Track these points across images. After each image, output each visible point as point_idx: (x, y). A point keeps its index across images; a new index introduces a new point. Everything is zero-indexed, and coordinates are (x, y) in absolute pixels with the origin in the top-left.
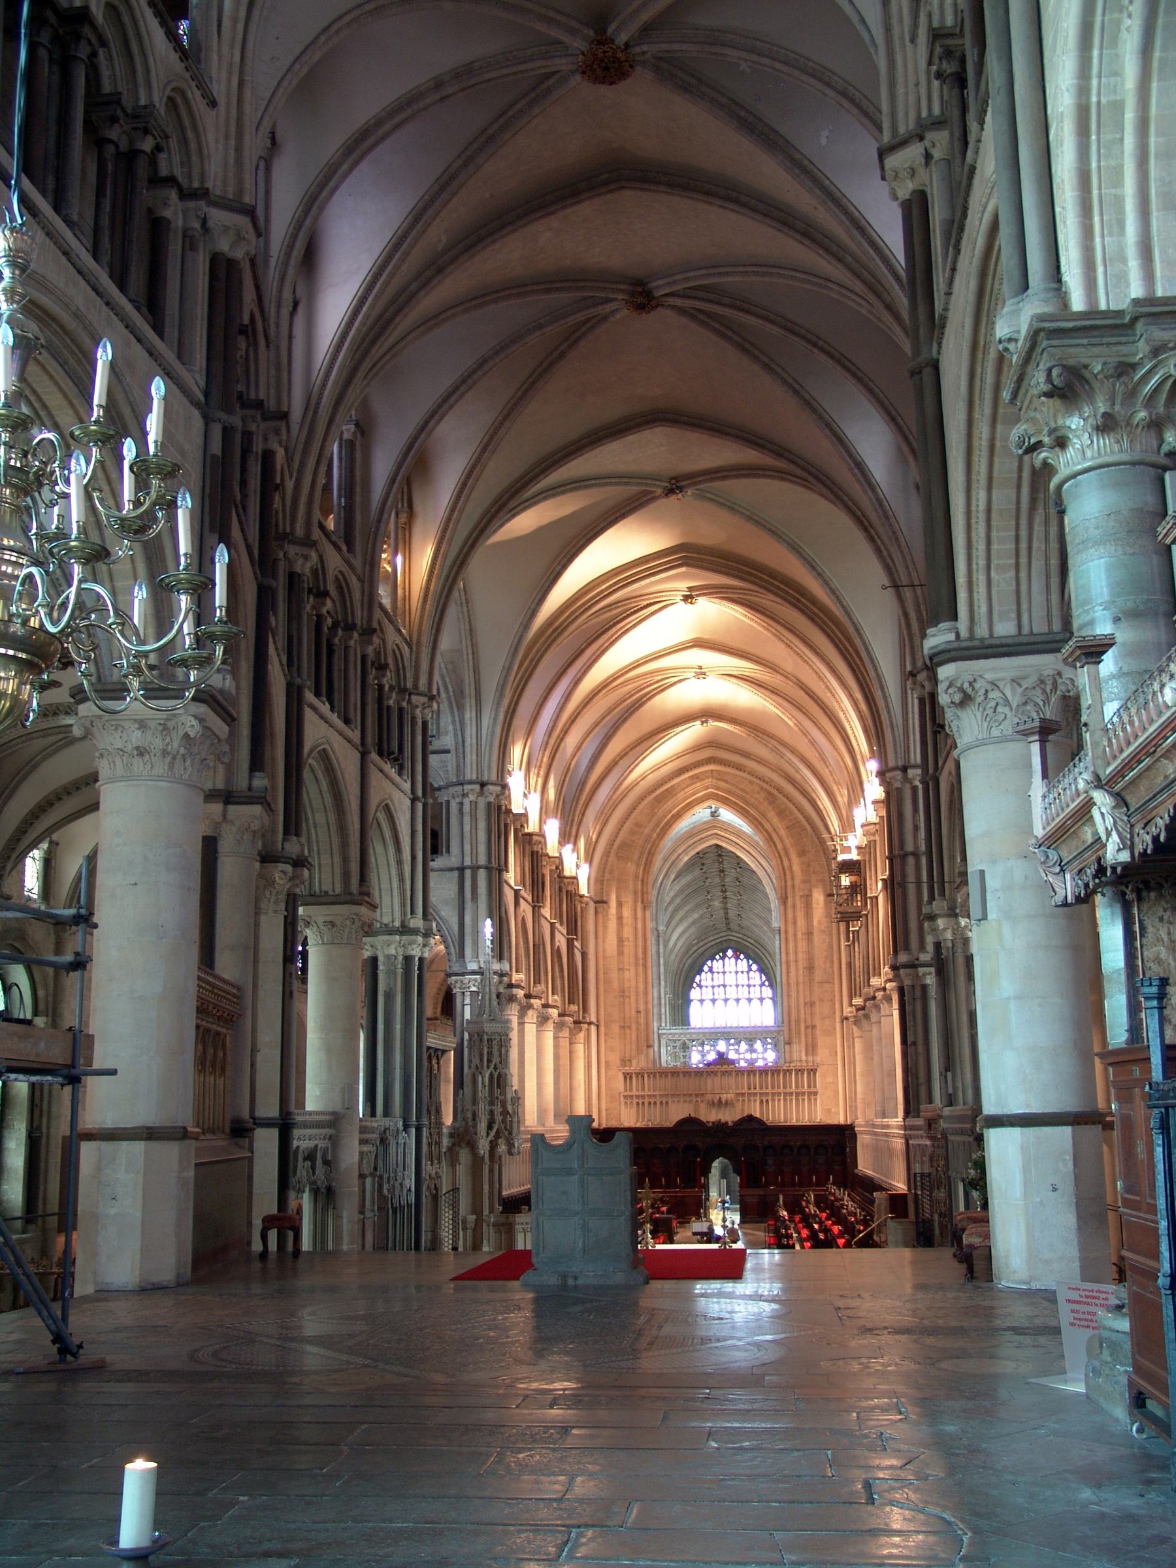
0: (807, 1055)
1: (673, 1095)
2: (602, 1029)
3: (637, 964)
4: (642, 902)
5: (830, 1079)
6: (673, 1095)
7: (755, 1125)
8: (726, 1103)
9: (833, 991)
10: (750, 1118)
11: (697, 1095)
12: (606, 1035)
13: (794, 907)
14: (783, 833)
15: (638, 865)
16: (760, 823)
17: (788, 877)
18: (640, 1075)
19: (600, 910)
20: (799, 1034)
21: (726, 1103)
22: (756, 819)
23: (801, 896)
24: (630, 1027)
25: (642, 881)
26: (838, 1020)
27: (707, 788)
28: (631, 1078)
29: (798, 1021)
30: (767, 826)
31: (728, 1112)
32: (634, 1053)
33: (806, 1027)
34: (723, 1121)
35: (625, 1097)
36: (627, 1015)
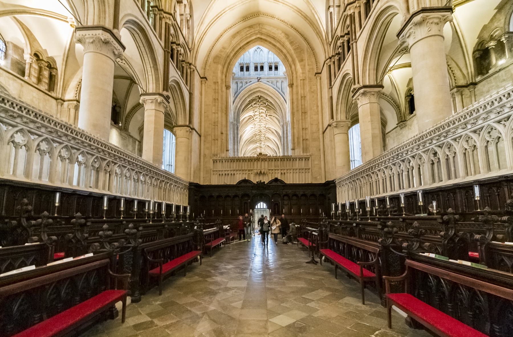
0: (303, 152)
2: (202, 138)
3: (222, 112)
4: (226, 86)
5: (316, 162)
7: (279, 184)
8: (264, 173)
9: (318, 120)
10: (276, 180)
11: (249, 171)
12: (204, 141)
13: (297, 86)
14: (292, 52)
15: (224, 67)
16: (282, 51)
17: (294, 73)
18: (221, 161)
19: (203, 82)
20: (299, 143)
21: (264, 173)
22: (280, 49)
23: (301, 80)
24: (217, 140)
25: (226, 76)
28: (217, 162)
29: (298, 138)
30: (284, 51)
31: (265, 178)
32: (219, 152)
33: (303, 140)
34: (262, 181)
35: (213, 171)
36: (216, 134)
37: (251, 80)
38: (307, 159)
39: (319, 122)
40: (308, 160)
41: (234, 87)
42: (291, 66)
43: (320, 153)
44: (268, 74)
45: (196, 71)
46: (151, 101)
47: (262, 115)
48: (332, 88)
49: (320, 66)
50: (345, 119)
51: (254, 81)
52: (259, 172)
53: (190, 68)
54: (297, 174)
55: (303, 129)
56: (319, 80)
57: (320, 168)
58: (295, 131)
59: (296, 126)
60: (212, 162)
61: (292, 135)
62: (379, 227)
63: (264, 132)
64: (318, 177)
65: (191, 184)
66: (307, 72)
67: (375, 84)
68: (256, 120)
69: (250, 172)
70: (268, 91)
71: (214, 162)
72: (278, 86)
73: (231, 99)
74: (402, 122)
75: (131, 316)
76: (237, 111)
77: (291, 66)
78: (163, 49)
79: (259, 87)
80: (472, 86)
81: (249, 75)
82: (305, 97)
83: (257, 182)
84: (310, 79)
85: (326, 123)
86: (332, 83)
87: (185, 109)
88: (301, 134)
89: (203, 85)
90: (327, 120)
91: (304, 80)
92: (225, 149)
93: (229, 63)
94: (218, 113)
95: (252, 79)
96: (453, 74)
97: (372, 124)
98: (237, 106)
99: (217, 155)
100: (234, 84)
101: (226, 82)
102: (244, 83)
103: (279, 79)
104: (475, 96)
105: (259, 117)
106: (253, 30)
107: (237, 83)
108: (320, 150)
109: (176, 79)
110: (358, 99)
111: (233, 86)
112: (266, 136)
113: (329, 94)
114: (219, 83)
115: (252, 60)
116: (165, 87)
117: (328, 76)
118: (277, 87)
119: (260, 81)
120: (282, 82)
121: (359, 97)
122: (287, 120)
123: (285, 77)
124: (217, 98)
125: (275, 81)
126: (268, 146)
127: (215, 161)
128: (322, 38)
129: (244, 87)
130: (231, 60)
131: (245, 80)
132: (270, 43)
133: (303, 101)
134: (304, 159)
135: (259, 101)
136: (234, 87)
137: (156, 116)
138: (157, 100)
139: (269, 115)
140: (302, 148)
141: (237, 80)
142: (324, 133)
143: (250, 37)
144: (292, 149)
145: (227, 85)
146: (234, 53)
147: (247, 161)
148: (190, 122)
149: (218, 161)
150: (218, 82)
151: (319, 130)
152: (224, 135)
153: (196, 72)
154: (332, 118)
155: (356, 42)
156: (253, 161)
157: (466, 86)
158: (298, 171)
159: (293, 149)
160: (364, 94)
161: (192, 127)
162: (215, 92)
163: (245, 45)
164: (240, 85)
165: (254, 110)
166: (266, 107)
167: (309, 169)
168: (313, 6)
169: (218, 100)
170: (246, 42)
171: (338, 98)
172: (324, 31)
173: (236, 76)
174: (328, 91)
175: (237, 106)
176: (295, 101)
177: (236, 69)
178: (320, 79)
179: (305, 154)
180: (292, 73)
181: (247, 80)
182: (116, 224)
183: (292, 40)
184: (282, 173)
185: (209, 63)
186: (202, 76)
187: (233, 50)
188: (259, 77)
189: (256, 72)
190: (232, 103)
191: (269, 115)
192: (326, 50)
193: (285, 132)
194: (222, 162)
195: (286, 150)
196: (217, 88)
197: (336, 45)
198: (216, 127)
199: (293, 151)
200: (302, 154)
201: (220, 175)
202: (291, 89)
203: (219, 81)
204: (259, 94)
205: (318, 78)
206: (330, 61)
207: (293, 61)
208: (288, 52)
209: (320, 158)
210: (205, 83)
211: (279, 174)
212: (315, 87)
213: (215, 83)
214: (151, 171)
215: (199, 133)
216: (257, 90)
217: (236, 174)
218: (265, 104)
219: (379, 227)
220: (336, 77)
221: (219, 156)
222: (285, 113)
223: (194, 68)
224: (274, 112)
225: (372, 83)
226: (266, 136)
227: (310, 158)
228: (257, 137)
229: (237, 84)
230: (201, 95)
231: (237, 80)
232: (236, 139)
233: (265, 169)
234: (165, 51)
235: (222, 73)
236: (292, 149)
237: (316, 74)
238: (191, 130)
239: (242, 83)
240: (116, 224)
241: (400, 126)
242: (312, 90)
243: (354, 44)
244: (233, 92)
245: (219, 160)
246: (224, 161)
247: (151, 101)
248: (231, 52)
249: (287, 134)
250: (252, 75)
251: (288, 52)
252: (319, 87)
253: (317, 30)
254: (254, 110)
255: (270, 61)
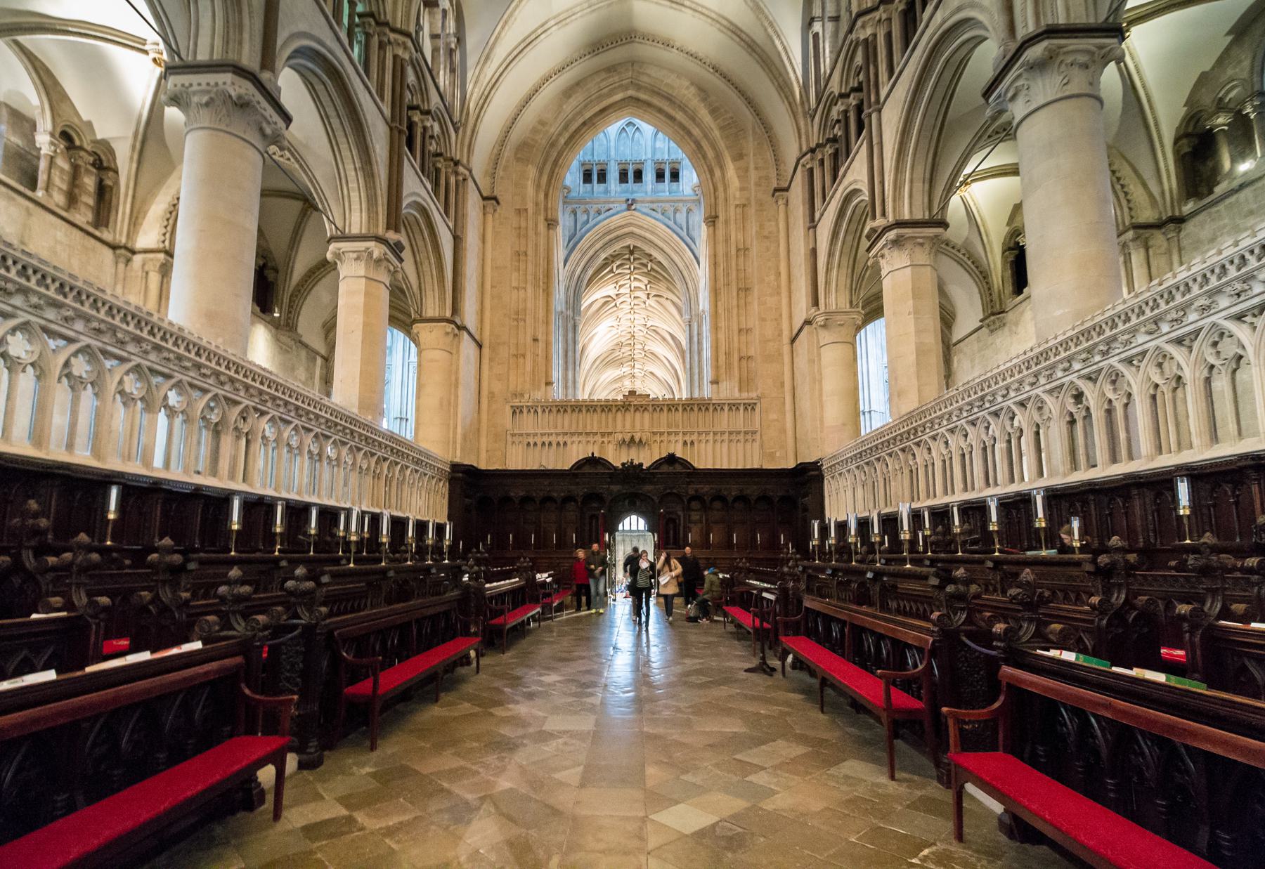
0: (740, 390)
1: (572, 434)
2: (486, 350)
3: (536, 286)
4: (546, 220)
5: (773, 416)
6: (572, 434)
7: (678, 468)
8: (640, 441)
9: (778, 309)
10: (671, 459)
11: (603, 435)
12: (491, 360)
13: (727, 222)
15: (541, 173)
16: (689, 133)
17: (721, 189)
18: (533, 409)
19: (490, 210)
20: (729, 366)
21: (640, 441)
23: (737, 206)
24: (524, 356)
25: (546, 195)
26: (786, 339)
27: (627, 89)
28: (521, 411)
30: (696, 132)
32: (527, 386)
33: (741, 359)
34: (636, 462)
35: (513, 435)
37: (611, 206)
38: (750, 407)
39: (781, 315)
40: (753, 409)
41: (567, 223)
42: (711, 172)
43: (784, 393)
44: (654, 191)
45: (470, 180)
46: (355, 255)
47: (638, 294)
48: (815, 227)
49: (785, 171)
50: (848, 305)
51: (619, 209)
52: (627, 439)
53: (457, 173)
54: (725, 445)
55: (740, 331)
56: (782, 208)
57: (783, 431)
58: (721, 336)
59: (722, 324)
60: (509, 411)
61: (711, 347)
62: (934, 581)
63: (642, 339)
64: (778, 454)
65: (455, 467)
66: (753, 187)
67: (927, 217)
68: (622, 306)
69: (605, 440)
70: (653, 233)
71: (514, 412)
72: (679, 221)
73: (560, 253)
74: (993, 314)
75: (296, 803)
76: (574, 283)
77: (711, 172)
78: (387, 123)
79: (630, 224)
80: (1171, 226)
81: (607, 191)
82: (746, 249)
83: (623, 464)
84: (760, 204)
85: (800, 316)
86: (817, 215)
87: (443, 277)
88: (736, 345)
89: (489, 217)
90: (802, 309)
91: (744, 206)
92: (544, 381)
93: (556, 163)
94: (525, 289)
95: (613, 202)
96: (1126, 194)
97: (916, 319)
98: (573, 272)
99: (522, 395)
100: (567, 215)
101: (546, 209)
102: (592, 213)
103: (681, 205)
104: (1180, 250)
105: (629, 300)
106: (616, 78)
107: (574, 212)
108: (782, 384)
109: (419, 200)
110: (882, 256)
111: (565, 221)
112: (646, 348)
113: (807, 243)
114: (530, 211)
115: (613, 153)
116: (393, 221)
117: (807, 196)
118: (675, 223)
119: (633, 207)
120: (689, 211)
121: (886, 251)
122: (701, 308)
123: (696, 198)
124: (523, 249)
125: (672, 209)
126: (651, 373)
127: (517, 411)
128: (791, 100)
129: (591, 223)
130: (560, 154)
131: (595, 206)
132: (660, 111)
133: (741, 260)
134: (742, 408)
135: (629, 259)
136: (567, 223)
137: (367, 294)
138: (371, 254)
139: (655, 296)
140: (737, 379)
141: (575, 206)
142: (793, 341)
143: (610, 95)
144: (713, 382)
145: (549, 217)
146: (567, 135)
147: (599, 410)
148: (455, 309)
149: (525, 410)
150: (526, 210)
151: (780, 335)
152: (541, 345)
153: (470, 183)
154: (816, 303)
155: (880, 111)
156: (614, 409)
157: (1158, 226)
158: (726, 437)
159: (715, 382)
160: (897, 243)
161: (459, 323)
162: (519, 236)
163: (596, 115)
164: (582, 218)
165: (616, 283)
166: (647, 274)
167: (754, 432)
168: (771, 19)
169: (526, 255)
170: (597, 108)
171: (831, 254)
172: (798, 82)
173: (573, 194)
174: (807, 236)
175: (573, 272)
176: (721, 259)
177: (572, 177)
178: (787, 204)
179: (745, 395)
180: (715, 190)
181: (599, 206)
182: (263, 567)
183: (717, 104)
184: (685, 443)
185: (503, 162)
186: (485, 194)
187: (566, 128)
188: (631, 197)
189: (624, 185)
190: (561, 264)
191: (655, 296)
192: (803, 131)
193: (695, 339)
194: (536, 411)
195: (696, 384)
196: (523, 224)
197: (827, 117)
198: (522, 323)
199: (715, 386)
200: (737, 395)
201: (529, 444)
202: (711, 228)
203: (530, 207)
204: (629, 242)
205: (780, 202)
206: (812, 159)
207: (719, 157)
208: (706, 136)
209: (784, 404)
210: (495, 210)
211: (680, 445)
212: (773, 223)
213: (519, 211)
214: (355, 434)
215: (477, 337)
216: (626, 230)
217: (569, 443)
218: (646, 266)
219: (934, 581)
220: (827, 199)
221: (527, 396)
222: (696, 290)
223: (467, 173)
224: (668, 288)
225: (918, 216)
226: (646, 348)
227: (758, 405)
228: (623, 350)
229: (575, 215)
230: (484, 242)
231: (575, 206)
232: (570, 354)
233: (642, 431)
234: (391, 129)
235: (538, 186)
236: (713, 382)
237: (776, 190)
238: (456, 331)
239: (586, 212)
240: (263, 567)
241: (989, 326)
242: (766, 233)
243: (874, 116)
244: (564, 236)
245: (527, 407)
246: (539, 410)
247: (355, 255)
248: (560, 134)
249: (700, 343)
250: (613, 194)
251: (706, 136)
252: (782, 225)
253: (780, 80)
254: (616, 283)
255: (659, 157)
